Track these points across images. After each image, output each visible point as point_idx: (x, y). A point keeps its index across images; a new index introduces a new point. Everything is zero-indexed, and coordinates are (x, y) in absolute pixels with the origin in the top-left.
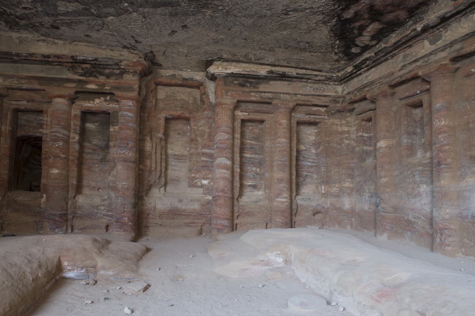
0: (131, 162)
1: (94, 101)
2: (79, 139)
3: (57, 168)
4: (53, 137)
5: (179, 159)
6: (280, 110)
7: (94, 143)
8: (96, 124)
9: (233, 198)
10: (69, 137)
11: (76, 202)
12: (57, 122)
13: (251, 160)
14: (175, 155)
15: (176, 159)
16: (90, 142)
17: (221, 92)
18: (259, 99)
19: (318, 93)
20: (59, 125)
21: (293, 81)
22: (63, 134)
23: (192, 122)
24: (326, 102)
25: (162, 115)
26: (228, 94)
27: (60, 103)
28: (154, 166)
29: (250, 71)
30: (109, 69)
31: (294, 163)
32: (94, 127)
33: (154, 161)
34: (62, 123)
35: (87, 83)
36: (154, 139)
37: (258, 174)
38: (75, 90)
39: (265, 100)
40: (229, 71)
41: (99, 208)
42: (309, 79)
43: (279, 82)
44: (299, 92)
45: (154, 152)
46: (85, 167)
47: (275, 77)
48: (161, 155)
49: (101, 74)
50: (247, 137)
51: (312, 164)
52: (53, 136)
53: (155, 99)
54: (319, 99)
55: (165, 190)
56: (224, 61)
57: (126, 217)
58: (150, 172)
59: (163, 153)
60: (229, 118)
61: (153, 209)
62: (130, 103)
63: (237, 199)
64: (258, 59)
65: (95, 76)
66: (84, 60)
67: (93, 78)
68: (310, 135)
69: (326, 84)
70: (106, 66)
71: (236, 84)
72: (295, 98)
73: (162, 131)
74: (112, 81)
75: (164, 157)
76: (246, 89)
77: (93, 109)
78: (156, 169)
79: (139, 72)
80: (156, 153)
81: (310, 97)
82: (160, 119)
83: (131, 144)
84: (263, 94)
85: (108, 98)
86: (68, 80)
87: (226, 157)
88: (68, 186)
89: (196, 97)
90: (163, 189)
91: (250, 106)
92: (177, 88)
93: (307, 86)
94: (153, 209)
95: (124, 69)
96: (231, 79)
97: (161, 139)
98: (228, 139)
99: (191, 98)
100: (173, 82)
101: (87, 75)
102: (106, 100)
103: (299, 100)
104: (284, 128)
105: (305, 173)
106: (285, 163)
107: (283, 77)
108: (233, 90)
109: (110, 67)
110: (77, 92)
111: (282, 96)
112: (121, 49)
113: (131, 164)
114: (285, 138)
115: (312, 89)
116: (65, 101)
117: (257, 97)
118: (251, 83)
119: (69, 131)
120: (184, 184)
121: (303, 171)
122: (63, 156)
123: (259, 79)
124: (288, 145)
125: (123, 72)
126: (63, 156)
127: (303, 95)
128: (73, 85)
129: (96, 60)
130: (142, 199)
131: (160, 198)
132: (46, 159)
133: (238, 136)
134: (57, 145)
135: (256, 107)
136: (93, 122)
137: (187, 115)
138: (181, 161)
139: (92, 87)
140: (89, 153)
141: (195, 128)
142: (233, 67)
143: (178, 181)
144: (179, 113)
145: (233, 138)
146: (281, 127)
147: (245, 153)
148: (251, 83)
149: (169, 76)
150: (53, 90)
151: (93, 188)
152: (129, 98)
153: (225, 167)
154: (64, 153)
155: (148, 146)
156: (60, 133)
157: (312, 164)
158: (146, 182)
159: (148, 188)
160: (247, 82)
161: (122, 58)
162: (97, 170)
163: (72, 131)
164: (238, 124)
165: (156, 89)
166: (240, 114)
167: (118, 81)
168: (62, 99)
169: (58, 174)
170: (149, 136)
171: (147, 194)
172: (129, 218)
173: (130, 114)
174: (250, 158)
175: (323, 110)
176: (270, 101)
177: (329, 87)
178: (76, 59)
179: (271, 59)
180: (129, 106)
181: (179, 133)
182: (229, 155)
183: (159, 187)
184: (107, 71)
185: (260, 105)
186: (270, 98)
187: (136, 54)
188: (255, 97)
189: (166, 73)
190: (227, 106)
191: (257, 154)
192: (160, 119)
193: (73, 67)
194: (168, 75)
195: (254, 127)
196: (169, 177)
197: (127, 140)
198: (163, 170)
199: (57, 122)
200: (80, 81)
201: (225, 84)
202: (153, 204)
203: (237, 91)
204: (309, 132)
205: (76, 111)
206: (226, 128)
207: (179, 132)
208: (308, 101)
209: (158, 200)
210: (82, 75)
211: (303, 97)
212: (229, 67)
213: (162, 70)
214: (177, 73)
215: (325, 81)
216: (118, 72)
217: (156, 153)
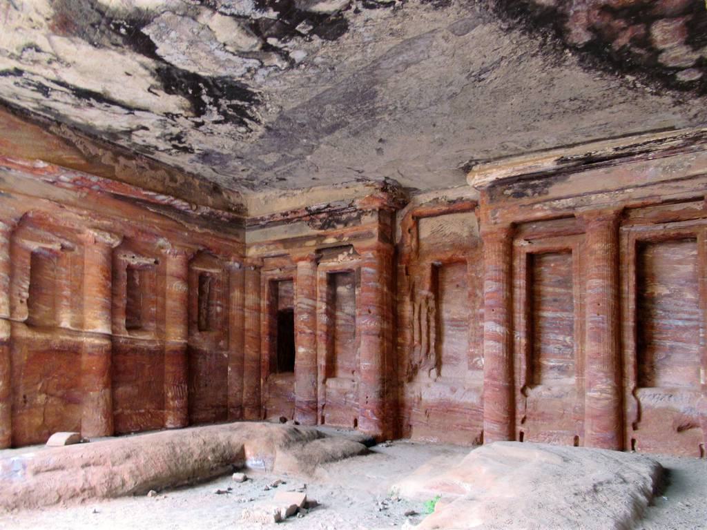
0: (374, 335)
1: (337, 257)
2: (327, 310)
3: (303, 346)
5: (458, 326)
6: (592, 226)
7: (346, 311)
8: (348, 287)
9: (511, 389)
10: (315, 308)
11: (326, 387)
13: (554, 321)
14: (453, 320)
15: (455, 326)
16: (341, 310)
17: (486, 214)
18: (549, 213)
19: (675, 175)
21: (615, 165)
22: (308, 305)
23: (468, 265)
24: (698, 190)
25: (427, 263)
26: (497, 215)
27: (304, 267)
28: (416, 337)
29: (524, 169)
30: (347, 213)
31: (629, 323)
32: (346, 290)
33: (416, 331)
34: (306, 292)
35: (325, 237)
36: (418, 298)
37: (568, 346)
38: (315, 248)
39: (559, 213)
40: (492, 178)
41: (348, 395)
42: (648, 152)
43: (587, 173)
44: (629, 184)
45: (416, 316)
46: (338, 343)
47: (575, 166)
48: (428, 321)
49: (338, 222)
50: (546, 281)
51: (687, 324)
53: (415, 240)
54: (677, 187)
55: (439, 374)
56: (485, 163)
57: (369, 409)
58: (413, 348)
59: (432, 319)
60: (499, 255)
61: (416, 401)
62: (370, 255)
63: (523, 391)
64: (529, 146)
65: (334, 227)
66: (318, 209)
67: (330, 230)
68: (680, 262)
69: (692, 151)
70: (341, 212)
71: (509, 196)
72: (621, 196)
73: (428, 286)
74: (350, 230)
75: (433, 324)
76: (525, 200)
77: (338, 269)
78: (420, 342)
79: (377, 210)
80: (419, 319)
81: (655, 187)
82: (423, 269)
83: (373, 310)
84: (555, 204)
85: (351, 252)
86: (309, 238)
87: (495, 321)
88: (317, 367)
89: (472, 225)
90: (434, 372)
91: (541, 227)
92: (446, 217)
93: (647, 166)
94: (416, 401)
95: (361, 210)
96: (499, 189)
97: (427, 299)
98: (497, 291)
99: (466, 229)
100: (436, 209)
101: (326, 226)
102: (349, 255)
103: (630, 198)
104: (598, 259)
105: (668, 343)
106: (601, 325)
107: (590, 162)
108: (503, 208)
109: (345, 211)
110: (318, 251)
111: (593, 197)
112: (355, 183)
113: (373, 338)
114: (600, 278)
115: (661, 169)
117: (545, 210)
118: (534, 187)
119: (315, 300)
120: (464, 365)
121: (664, 339)
122: (309, 331)
123: (546, 177)
124: (610, 291)
125: (362, 212)
126: (309, 331)
127: (637, 187)
128: (313, 243)
129: (328, 206)
130: (403, 386)
131: (428, 386)
133: (520, 282)
135: (552, 227)
136: (345, 285)
137: (461, 257)
138: (461, 328)
139: (330, 241)
140: (342, 325)
141: (473, 274)
142: (495, 170)
143: (456, 359)
144: (450, 255)
145: (511, 287)
146: (593, 257)
147: (544, 310)
148: (534, 187)
149: (430, 202)
150: (296, 252)
151: (347, 370)
152: (368, 249)
153: (496, 338)
154: (309, 328)
155: (407, 310)
157: (687, 324)
158: (406, 362)
159: (411, 370)
160: (526, 187)
161: (357, 195)
162: (350, 346)
163: (319, 299)
164: (520, 264)
165: (417, 223)
166: (523, 246)
167: (355, 228)
169: (304, 353)
170: (409, 294)
171: (410, 380)
172: (373, 411)
173: (370, 270)
174: (554, 318)
175: (698, 206)
176: (571, 212)
177: (704, 154)
178: (310, 211)
179: (552, 141)
180: (369, 258)
181: (458, 286)
182: (502, 317)
183: (427, 369)
184: (344, 217)
185: (559, 221)
186: (569, 208)
187: (372, 185)
188: (543, 210)
189: (423, 199)
190: (494, 235)
191: (566, 311)
192: (423, 269)
193: (312, 220)
194: (428, 200)
195: (558, 263)
196: (444, 354)
197: (368, 306)
198: (433, 344)
200: (319, 236)
201: (491, 199)
202: (417, 394)
203: (510, 207)
204: (680, 257)
205: (321, 275)
206: (494, 273)
207: (458, 283)
208: (651, 196)
209: (426, 389)
210: (322, 228)
211: (639, 190)
212: (489, 171)
213: (421, 196)
214: (440, 195)
215: (686, 145)
216: (355, 215)
217: (419, 319)
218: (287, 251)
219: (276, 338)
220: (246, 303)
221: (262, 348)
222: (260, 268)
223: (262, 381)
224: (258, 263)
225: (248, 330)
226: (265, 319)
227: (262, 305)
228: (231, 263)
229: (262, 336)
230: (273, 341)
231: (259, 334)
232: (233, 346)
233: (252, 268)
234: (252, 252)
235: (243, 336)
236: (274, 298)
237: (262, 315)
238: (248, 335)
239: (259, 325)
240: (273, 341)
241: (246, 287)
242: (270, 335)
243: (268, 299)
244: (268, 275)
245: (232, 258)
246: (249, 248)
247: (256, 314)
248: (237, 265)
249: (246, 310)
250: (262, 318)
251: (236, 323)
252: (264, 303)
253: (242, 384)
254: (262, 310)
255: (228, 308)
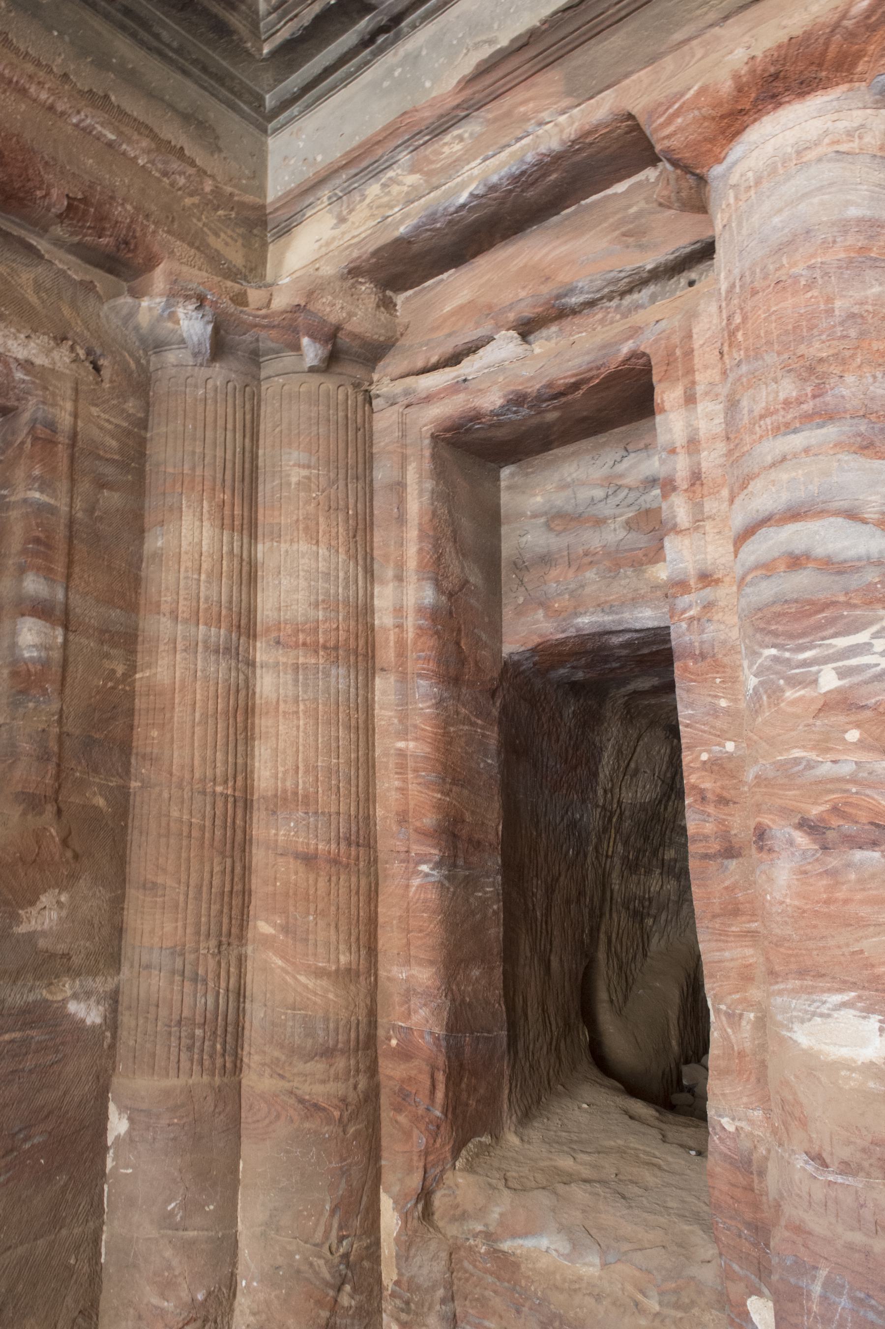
4: (766, 590)
12: (788, 388)
20: (828, 416)
52: (767, 568)
116: (858, 116)
132: (730, 852)
134: (829, 680)
156: (852, 515)
168: (817, 101)
199: (788, 388)
218: (600, 109)
219: (494, 862)
220: (267, 605)
221: (390, 940)
222: (373, 353)
223: (390, 1220)
224: (358, 313)
225: (282, 802)
226: (407, 717)
227: (383, 619)
228: (149, 307)
229: (384, 845)
230: (470, 883)
231: (361, 839)
232: (158, 928)
233: (312, 352)
234: (311, 252)
235: (236, 846)
236: (476, 578)
237: (384, 688)
238: (277, 836)
239: (366, 766)
240: (470, 883)
241: (266, 489)
242: (454, 838)
243: (436, 570)
244: (415, 404)
245: (159, 278)
246: (286, 230)
247: (341, 678)
248: (193, 326)
249: (262, 653)
250: (385, 714)
251: (177, 745)
252: (403, 599)
253: (226, 1248)
254: (387, 654)
255: (127, 641)
